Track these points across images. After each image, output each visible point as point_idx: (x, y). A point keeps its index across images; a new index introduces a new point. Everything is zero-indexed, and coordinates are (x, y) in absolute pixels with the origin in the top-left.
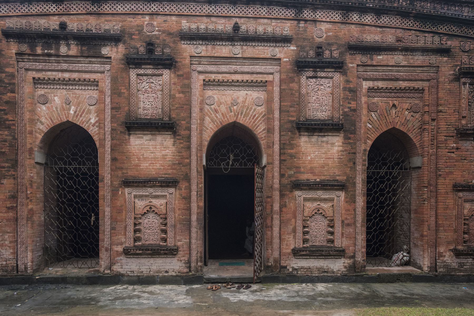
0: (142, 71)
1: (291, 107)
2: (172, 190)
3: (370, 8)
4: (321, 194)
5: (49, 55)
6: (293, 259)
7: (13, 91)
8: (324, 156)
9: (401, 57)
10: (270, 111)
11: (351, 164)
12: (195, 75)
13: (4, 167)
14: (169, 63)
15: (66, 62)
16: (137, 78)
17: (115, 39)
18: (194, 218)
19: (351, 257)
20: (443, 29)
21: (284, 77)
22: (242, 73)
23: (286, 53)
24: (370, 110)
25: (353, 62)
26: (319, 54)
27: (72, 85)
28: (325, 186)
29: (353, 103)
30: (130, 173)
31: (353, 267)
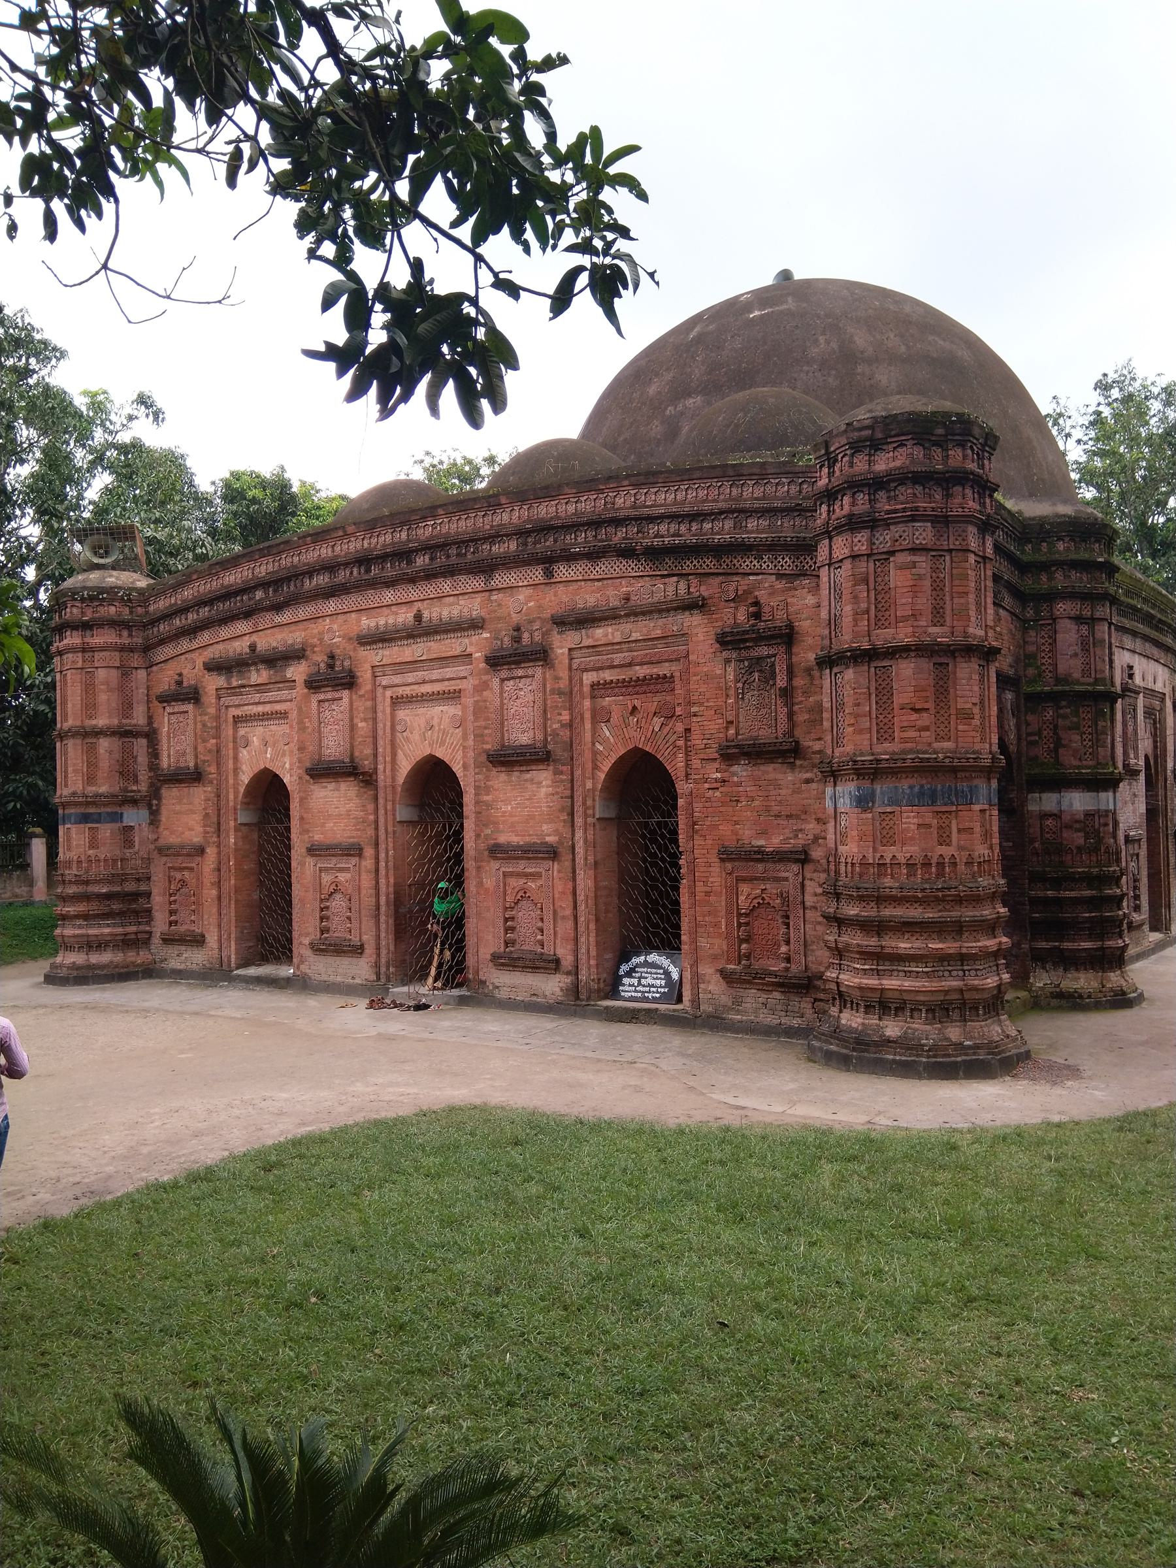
0: (322, 697)
1: (485, 728)
2: (354, 860)
3: (578, 554)
4: (521, 866)
5: (244, 686)
6: (493, 970)
8: (527, 803)
9: (629, 626)
10: (465, 737)
11: (564, 816)
12: (380, 690)
14: (349, 681)
15: (258, 692)
16: (319, 705)
17: (295, 655)
18: (383, 899)
19: (568, 973)
20: (689, 566)
22: (432, 681)
23: (477, 645)
24: (595, 721)
25: (562, 644)
26: (517, 640)
28: (530, 852)
29: (564, 712)
30: (317, 837)
31: (575, 991)
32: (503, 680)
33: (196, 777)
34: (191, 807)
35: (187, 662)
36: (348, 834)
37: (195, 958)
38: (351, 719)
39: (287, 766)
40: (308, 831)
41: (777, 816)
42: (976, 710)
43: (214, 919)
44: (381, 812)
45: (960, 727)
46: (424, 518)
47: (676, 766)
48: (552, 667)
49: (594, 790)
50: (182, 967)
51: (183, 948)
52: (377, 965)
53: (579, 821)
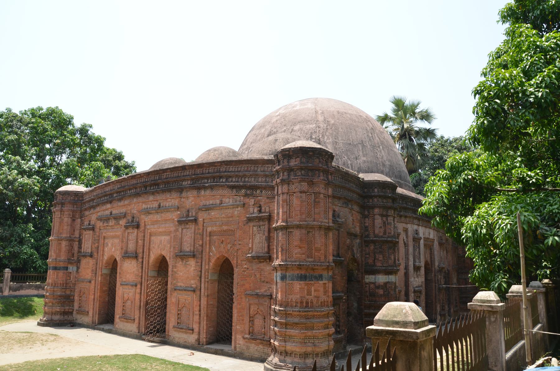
0: (129, 231)
5: (107, 226)
11: (198, 278)
12: (146, 230)
14: (138, 227)
26: (188, 216)
30: (124, 280)
31: (198, 340)
32: (182, 229)
33: (91, 256)
35: (93, 216)
36: (133, 279)
37: (86, 320)
38: (137, 239)
40: (121, 278)
41: (263, 282)
42: (323, 248)
43: (92, 306)
44: (144, 272)
45: (316, 254)
47: (234, 263)
48: (198, 224)
49: (208, 269)
52: (139, 327)
53: (203, 280)
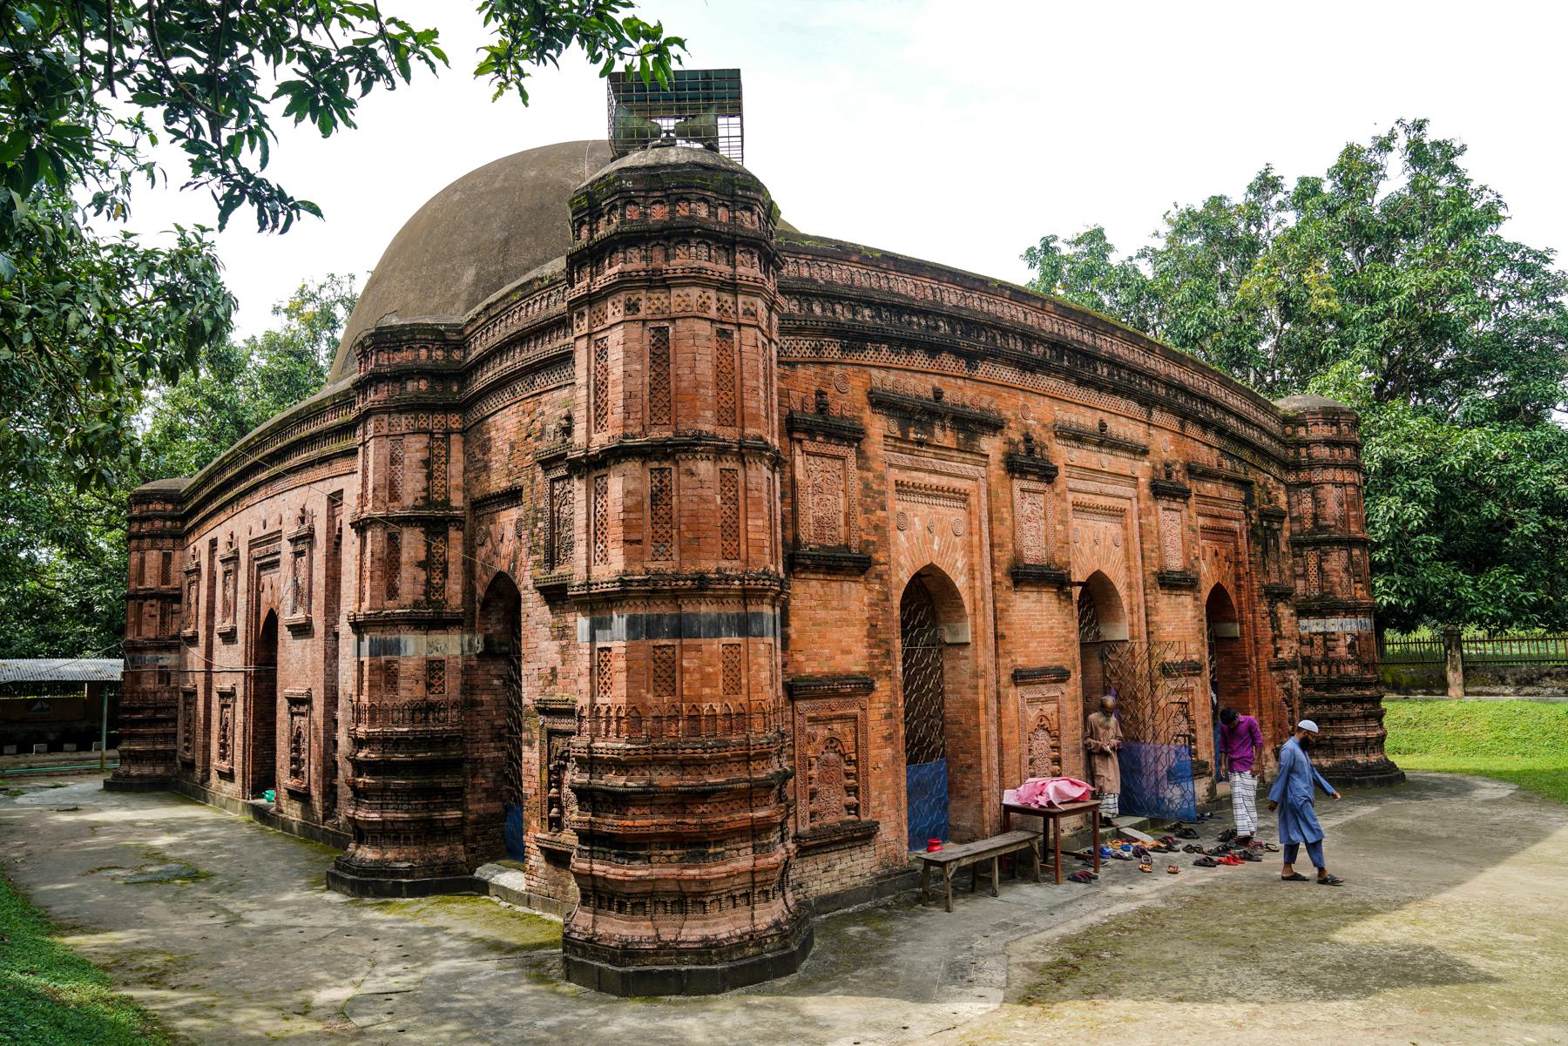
0: (1026, 485)
7: (883, 509)
13: (876, 657)
14: (1048, 474)
15: (936, 457)
17: (994, 425)
21: (1142, 506)
22: (1107, 495)
26: (1169, 475)
27: (937, 497)
30: (1021, 661)
34: (844, 614)
39: (959, 565)
46: (1105, 332)
50: (836, 888)
51: (835, 856)
